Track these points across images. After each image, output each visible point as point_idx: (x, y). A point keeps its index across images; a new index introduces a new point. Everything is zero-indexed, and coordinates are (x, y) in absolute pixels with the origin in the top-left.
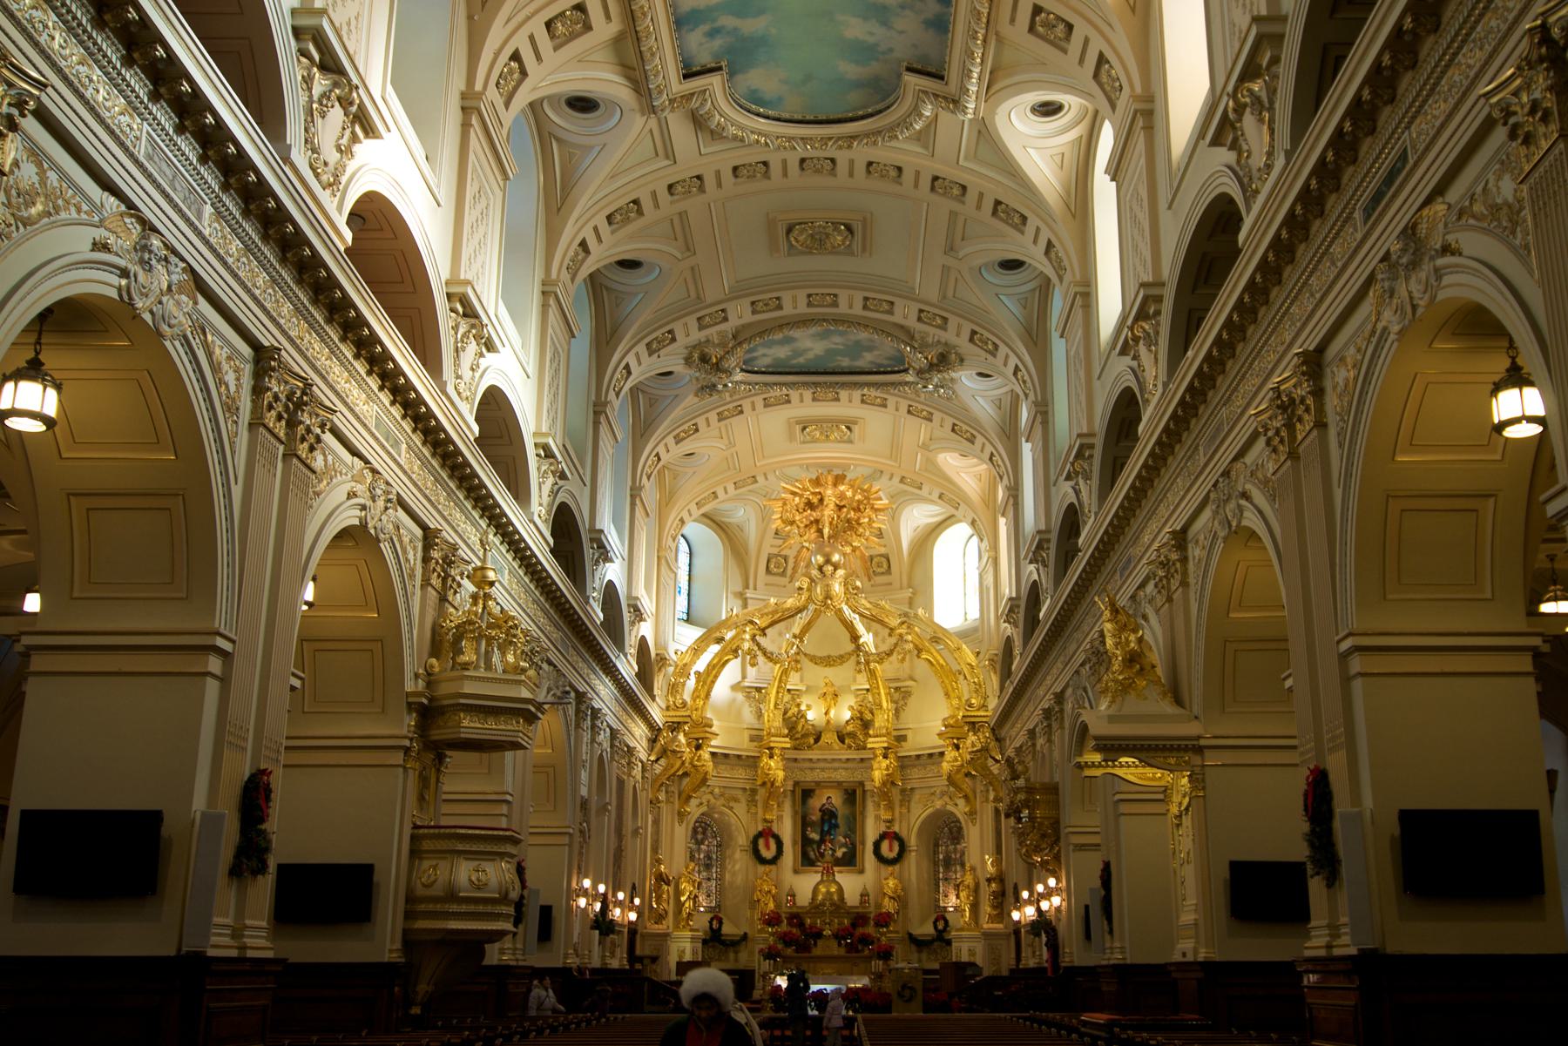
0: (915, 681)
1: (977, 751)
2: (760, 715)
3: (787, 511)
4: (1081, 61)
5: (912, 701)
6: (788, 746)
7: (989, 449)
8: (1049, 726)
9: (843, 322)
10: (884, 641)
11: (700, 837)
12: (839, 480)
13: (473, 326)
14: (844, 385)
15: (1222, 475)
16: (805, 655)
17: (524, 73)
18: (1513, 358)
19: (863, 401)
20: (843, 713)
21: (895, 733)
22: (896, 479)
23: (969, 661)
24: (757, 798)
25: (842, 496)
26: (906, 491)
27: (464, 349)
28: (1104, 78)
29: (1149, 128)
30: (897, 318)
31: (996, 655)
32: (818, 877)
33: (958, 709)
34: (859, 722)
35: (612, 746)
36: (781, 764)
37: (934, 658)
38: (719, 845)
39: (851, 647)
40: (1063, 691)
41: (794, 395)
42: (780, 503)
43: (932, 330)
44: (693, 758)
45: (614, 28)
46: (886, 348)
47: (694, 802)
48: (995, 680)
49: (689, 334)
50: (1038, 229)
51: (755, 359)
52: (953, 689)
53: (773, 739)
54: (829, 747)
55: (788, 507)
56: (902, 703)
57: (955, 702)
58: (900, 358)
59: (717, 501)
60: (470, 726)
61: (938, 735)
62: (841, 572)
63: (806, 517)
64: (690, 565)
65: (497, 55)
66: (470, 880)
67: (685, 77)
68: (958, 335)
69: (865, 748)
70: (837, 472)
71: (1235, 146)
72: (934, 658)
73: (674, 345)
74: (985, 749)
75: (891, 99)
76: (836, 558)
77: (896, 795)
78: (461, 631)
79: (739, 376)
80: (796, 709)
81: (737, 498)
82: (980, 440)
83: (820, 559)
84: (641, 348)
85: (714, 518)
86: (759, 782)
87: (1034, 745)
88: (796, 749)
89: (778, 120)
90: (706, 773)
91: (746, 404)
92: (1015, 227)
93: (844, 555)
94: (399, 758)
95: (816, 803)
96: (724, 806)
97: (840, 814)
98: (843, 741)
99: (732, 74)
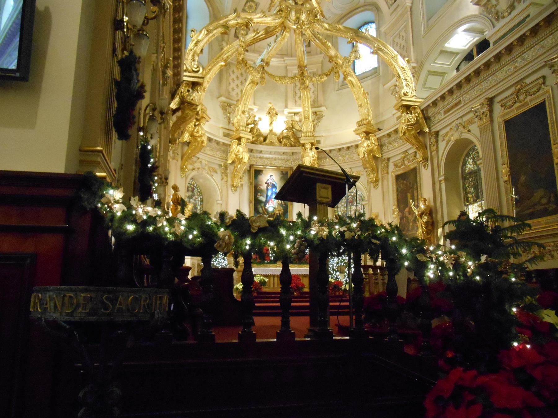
5: (323, 121)
6: (251, 137)
11: (190, 193)
16: (269, 74)
23: (402, 66)
24: (228, 171)
34: (291, 130)
36: (246, 150)
38: (202, 201)
53: (241, 131)
56: (317, 121)
61: (354, 131)
72: (356, 81)
86: (229, 161)
88: (253, 143)
90: (203, 142)
96: (207, 173)
98: (281, 142)
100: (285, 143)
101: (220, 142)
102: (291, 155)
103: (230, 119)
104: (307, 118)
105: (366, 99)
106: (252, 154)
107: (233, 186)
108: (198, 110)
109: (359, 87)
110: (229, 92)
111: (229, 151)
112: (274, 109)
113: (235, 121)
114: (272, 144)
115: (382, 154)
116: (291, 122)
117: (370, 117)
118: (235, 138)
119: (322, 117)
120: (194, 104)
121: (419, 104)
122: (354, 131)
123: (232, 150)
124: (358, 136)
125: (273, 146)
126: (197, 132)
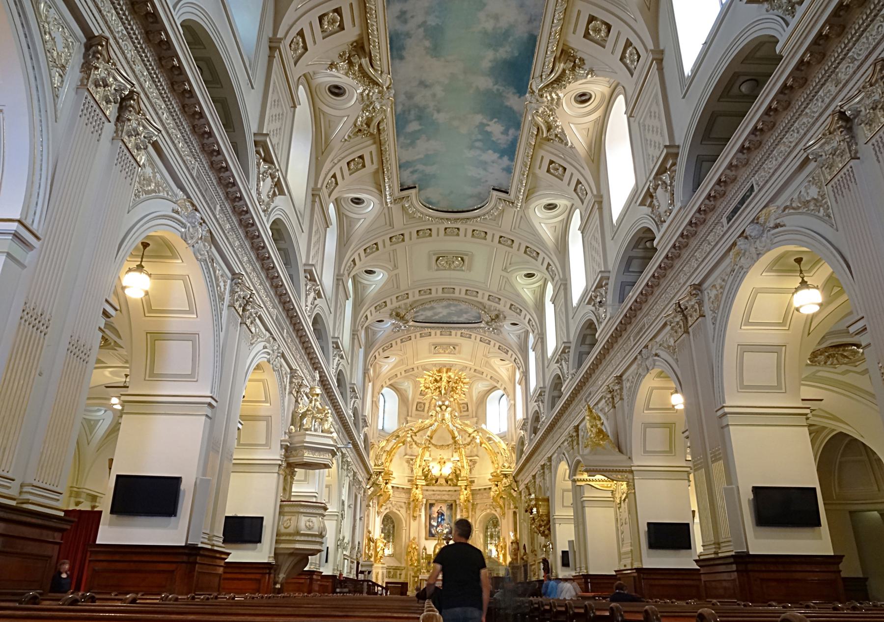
2: (412, 471)
4: (569, 184)
5: (477, 465)
7: (514, 356)
8: (544, 472)
9: (456, 300)
10: (465, 439)
11: (385, 523)
12: (448, 370)
13: (313, 285)
14: (454, 328)
15: (644, 347)
16: (433, 444)
17: (337, 184)
18: (803, 278)
19: (461, 336)
20: (447, 470)
22: (472, 370)
25: (449, 377)
26: (475, 376)
27: (309, 294)
28: (578, 190)
29: (600, 209)
30: (479, 299)
32: (436, 542)
35: (354, 479)
39: (451, 441)
40: (551, 457)
41: (433, 332)
43: (493, 304)
45: (375, 166)
46: (473, 313)
47: (384, 507)
48: (514, 456)
49: (393, 304)
50: (544, 258)
51: (418, 316)
54: (441, 485)
55: (427, 381)
57: (496, 466)
58: (480, 317)
60: (308, 456)
62: (449, 409)
65: (326, 175)
66: (306, 527)
67: (401, 190)
68: (505, 306)
69: (456, 485)
70: (448, 367)
71: (651, 205)
73: (386, 308)
74: (510, 485)
75: (485, 202)
76: (447, 403)
77: (470, 505)
78: (304, 415)
79: (411, 323)
81: (406, 377)
82: (510, 352)
83: (440, 403)
84: (373, 309)
85: (396, 386)
87: (535, 482)
88: (427, 485)
89: (437, 210)
91: (413, 336)
92: (533, 257)
93: (450, 402)
94: (276, 469)
95: (435, 509)
97: (445, 514)
99: (419, 190)
107: (413, 516)
114: (441, 485)
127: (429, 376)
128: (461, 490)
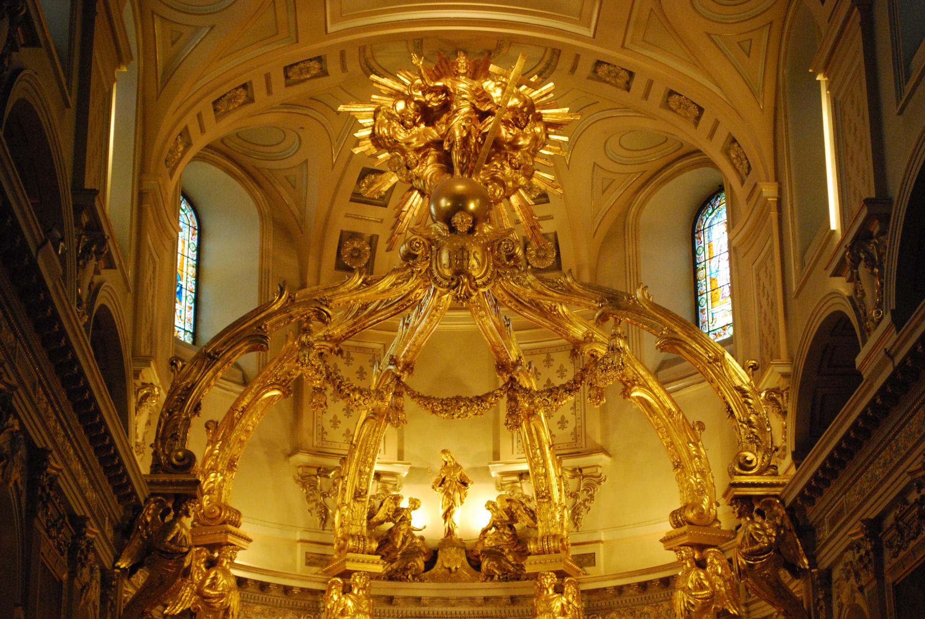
0: (610, 456)
1: (761, 551)
2: (325, 517)
3: (381, 124)
6: (379, 569)
21: (574, 551)
23: (738, 383)
31: (785, 376)
33: (702, 492)
37: (657, 398)
42: (371, 109)
44: (203, 582)
52: (691, 458)
53: (350, 555)
59: (250, 108)
61: (662, 541)
62: (487, 229)
63: (418, 135)
64: (199, 249)
69: (517, 575)
72: (657, 398)
80: (392, 506)
100: (488, 570)
101: (292, 588)
102: (507, 604)
103: (326, 511)
104: (543, 497)
105: (696, 445)
106: (392, 608)
108: (186, 565)
109: (670, 412)
110: (323, 432)
111: (322, 609)
112: (457, 466)
113: (337, 519)
114: (450, 575)
115: (746, 605)
116: (507, 505)
117: (706, 501)
118: (336, 574)
119: (599, 483)
120: (175, 553)
121: (781, 489)
122: (662, 541)
123: (329, 607)
124: (672, 552)
125: (454, 581)
126: (213, 585)
127: (397, 95)
128: (542, 588)
